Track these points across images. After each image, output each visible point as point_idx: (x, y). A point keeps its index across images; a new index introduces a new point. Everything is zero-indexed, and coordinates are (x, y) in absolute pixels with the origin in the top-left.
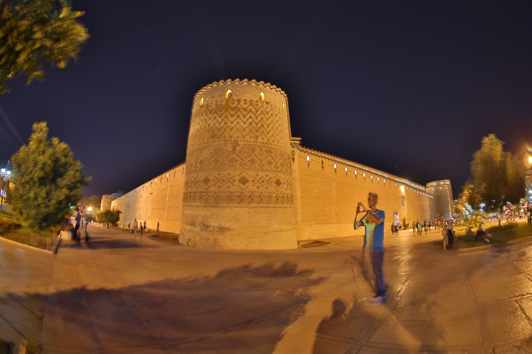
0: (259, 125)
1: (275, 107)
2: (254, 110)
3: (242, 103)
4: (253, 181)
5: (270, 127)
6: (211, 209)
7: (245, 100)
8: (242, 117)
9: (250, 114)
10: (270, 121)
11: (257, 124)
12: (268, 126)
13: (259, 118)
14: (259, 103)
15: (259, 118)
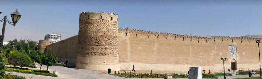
0: (99, 29)
1: (107, 20)
2: (97, 23)
3: (93, 21)
4: (96, 48)
5: (103, 29)
6: (83, 57)
7: (94, 20)
8: (93, 26)
9: (96, 25)
10: (103, 26)
11: (98, 29)
12: (102, 29)
13: (99, 26)
14: (99, 20)
15: (99, 26)
